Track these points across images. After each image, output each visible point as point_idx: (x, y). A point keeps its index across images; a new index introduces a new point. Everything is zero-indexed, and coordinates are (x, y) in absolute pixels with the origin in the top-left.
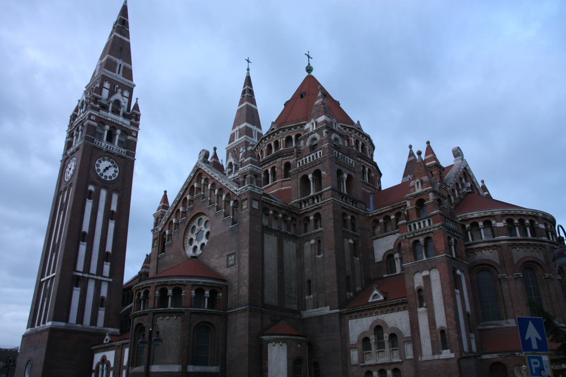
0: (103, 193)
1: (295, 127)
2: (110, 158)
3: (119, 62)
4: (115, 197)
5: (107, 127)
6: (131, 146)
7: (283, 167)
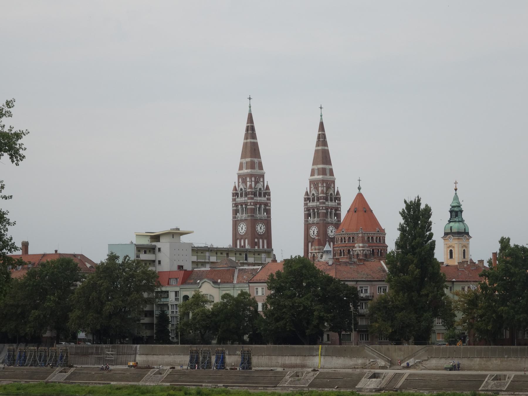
0: (261, 241)
1: (352, 234)
2: (261, 222)
3: (256, 160)
4: (265, 241)
5: (258, 206)
6: (268, 212)
7: (347, 251)
